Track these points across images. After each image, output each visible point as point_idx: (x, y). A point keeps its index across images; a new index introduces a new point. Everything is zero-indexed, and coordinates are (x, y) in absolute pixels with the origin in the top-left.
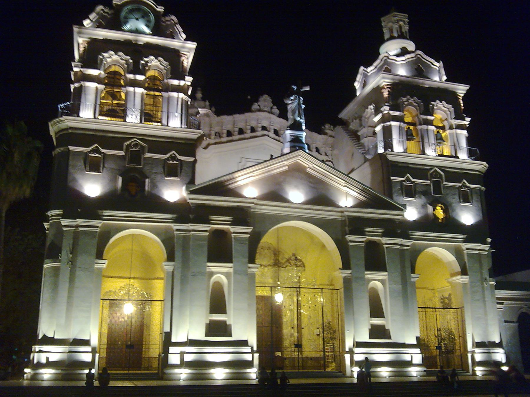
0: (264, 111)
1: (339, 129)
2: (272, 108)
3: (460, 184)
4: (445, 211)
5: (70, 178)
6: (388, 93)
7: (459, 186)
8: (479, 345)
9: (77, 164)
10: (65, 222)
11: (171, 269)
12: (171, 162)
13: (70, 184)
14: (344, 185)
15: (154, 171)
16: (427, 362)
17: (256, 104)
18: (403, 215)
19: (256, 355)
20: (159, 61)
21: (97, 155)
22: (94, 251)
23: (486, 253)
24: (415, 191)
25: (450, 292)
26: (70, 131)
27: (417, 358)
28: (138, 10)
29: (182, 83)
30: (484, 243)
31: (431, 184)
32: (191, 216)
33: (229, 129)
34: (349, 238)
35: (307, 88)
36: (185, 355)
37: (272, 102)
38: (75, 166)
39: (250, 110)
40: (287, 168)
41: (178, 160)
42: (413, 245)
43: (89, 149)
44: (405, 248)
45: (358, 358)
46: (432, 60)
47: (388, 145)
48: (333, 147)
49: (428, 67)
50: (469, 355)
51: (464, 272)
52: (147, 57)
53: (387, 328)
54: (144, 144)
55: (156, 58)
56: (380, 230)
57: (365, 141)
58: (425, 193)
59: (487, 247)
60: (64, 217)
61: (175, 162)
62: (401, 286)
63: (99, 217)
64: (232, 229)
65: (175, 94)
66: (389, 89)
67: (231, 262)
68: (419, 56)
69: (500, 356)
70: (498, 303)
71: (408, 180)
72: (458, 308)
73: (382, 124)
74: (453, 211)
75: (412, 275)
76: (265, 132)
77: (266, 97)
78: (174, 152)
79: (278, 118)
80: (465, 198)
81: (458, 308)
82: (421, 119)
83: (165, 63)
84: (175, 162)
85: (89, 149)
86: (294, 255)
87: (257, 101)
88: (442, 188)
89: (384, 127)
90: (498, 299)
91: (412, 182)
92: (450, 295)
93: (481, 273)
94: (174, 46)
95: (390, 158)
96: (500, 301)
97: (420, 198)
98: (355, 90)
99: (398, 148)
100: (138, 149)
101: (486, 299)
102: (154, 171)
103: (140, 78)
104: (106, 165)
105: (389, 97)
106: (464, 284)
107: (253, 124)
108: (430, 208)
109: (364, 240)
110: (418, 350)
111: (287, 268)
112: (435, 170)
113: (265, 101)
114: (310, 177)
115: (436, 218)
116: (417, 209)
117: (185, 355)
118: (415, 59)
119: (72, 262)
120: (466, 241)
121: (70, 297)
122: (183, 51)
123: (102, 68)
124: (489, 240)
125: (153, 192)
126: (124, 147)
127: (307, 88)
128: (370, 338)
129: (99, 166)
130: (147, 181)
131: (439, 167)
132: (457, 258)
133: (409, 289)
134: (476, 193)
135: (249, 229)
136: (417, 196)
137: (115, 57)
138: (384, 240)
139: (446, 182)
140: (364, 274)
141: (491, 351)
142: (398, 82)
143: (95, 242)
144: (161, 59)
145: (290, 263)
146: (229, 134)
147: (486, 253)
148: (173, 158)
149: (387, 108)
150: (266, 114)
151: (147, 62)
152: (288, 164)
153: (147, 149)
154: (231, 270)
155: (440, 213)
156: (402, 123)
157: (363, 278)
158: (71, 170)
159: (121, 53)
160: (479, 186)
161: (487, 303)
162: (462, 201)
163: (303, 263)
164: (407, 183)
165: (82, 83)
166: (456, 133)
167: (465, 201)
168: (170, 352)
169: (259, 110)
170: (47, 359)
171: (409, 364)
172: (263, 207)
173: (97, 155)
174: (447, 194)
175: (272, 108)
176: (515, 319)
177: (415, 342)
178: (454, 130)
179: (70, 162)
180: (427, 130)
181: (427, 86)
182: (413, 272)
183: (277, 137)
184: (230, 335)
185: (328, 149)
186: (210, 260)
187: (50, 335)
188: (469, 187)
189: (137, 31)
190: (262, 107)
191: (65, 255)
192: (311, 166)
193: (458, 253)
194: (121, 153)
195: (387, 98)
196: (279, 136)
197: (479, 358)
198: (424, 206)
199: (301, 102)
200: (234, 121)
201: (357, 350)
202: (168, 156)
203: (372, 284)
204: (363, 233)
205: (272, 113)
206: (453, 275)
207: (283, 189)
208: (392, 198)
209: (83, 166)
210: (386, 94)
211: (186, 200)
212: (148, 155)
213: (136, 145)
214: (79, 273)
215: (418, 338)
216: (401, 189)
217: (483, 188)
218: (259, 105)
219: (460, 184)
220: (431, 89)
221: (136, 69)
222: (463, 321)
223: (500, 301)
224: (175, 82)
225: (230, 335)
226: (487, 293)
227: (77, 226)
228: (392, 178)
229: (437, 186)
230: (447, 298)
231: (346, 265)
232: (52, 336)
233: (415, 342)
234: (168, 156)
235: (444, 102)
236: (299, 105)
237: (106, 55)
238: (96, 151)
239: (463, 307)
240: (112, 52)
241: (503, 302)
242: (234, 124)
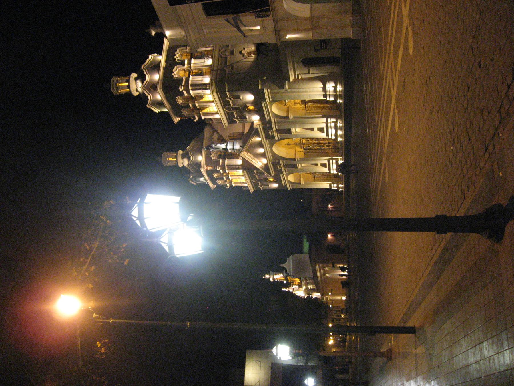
3: (230, 100)
9: (267, 188)
19: (333, 158)
20: (214, 175)
23: (269, 90)
30: (262, 91)
40: (249, 154)
44: (276, 121)
46: (149, 101)
59: (266, 92)
62: (297, 125)
94: (205, 173)
97: (245, 114)
109: (277, 134)
118: (153, 106)
120: (265, 100)
122: (205, 170)
123: (225, 183)
128: (324, 132)
131: (223, 108)
135: (281, 162)
147: (269, 90)
148: (256, 174)
151: (217, 177)
152: (246, 153)
156: (201, 115)
160: (227, 93)
162: (240, 99)
167: (239, 98)
172: (270, 158)
181: (170, 105)
184: (326, 164)
186: (297, 168)
189: (205, 179)
202: (256, 175)
212: (257, 178)
216: (243, 120)
225: (326, 164)
234: (256, 175)
237: (219, 184)
241: (297, 75)
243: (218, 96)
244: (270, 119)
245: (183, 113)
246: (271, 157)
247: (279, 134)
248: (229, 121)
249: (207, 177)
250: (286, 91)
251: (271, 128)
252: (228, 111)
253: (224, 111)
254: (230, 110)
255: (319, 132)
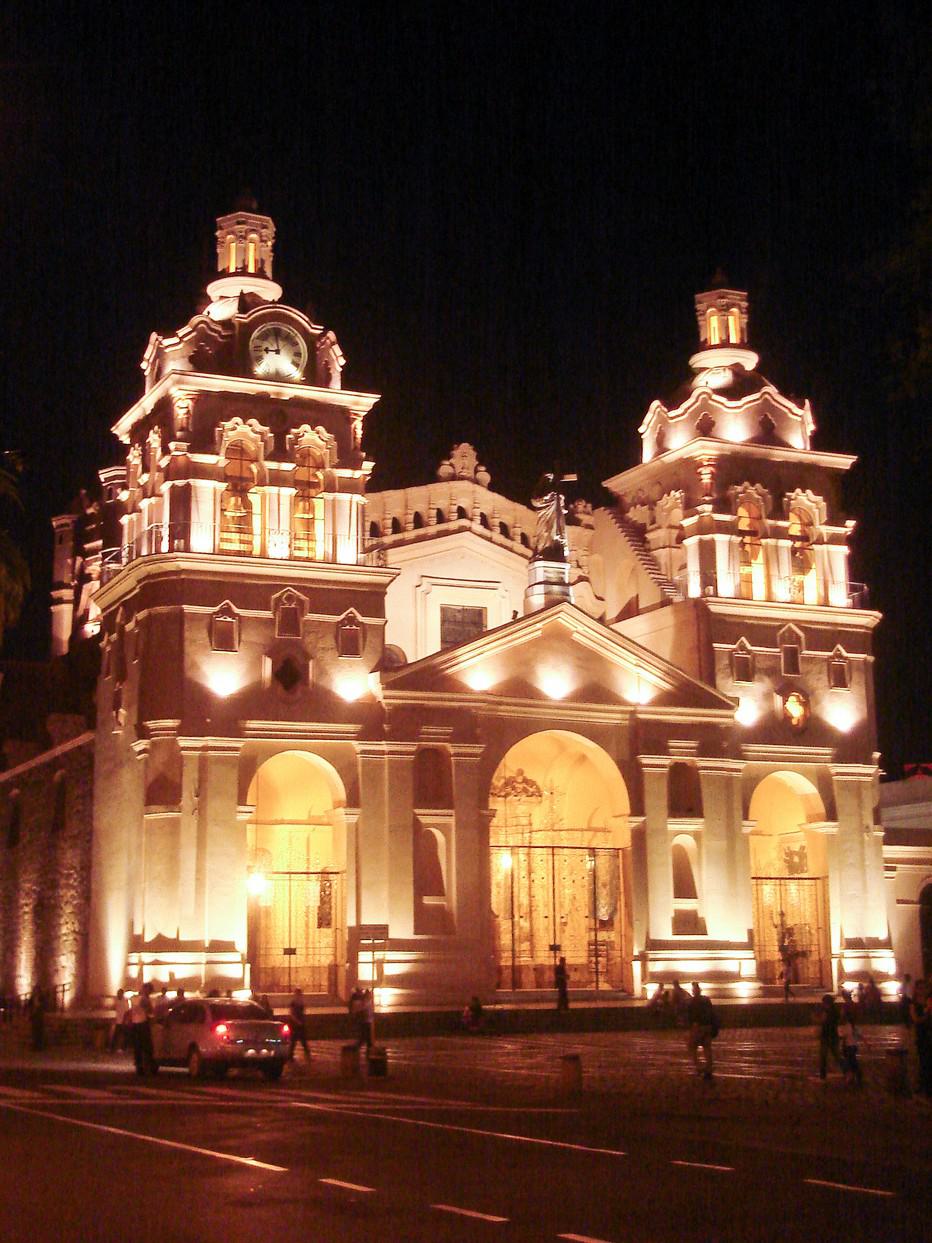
0: (462, 478)
1: (603, 517)
2: (476, 471)
3: (831, 654)
4: (806, 704)
5: (188, 662)
6: (710, 476)
7: (831, 657)
8: (854, 944)
9: (196, 639)
10: (183, 742)
11: (354, 819)
12: (348, 627)
13: (189, 674)
14: (634, 662)
15: (320, 645)
16: (764, 973)
17: (447, 463)
18: (732, 717)
21: (229, 619)
22: (234, 790)
24: (754, 666)
25: (804, 843)
26: (183, 576)
27: (749, 968)
28: (277, 334)
29: (357, 474)
30: (868, 761)
31: (782, 654)
32: (386, 727)
33: (397, 516)
34: (646, 760)
35: (573, 478)
36: (386, 966)
37: (478, 458)
38: (193, 641)
39: (436, 479)
40: (540, 632)
41: (359, 624)
42: (748, 768)
43: (217, 609)
44: (734, 774)
45: (655, 967)
47: (709, 579)
48: (591, 548)
49: (782, 417)
50: (834, 962)
51: (831, 814)
52: (297, 426)
53: (700, 915)
54: (303, 597)
55: (313, 429)
56: (693, 744)
57: (662, 555)
58: (771, 672)
59: (872, 769)
60: (182, 731)
61: (354, 627)
63: (239, 733)
64: (451, 749)
65: (345, 497)
66: (712, 469)
67: (450, 807)
68: (767, 396)
69: (885, 962)
70: (888, 869)
71: (743, 648)
72: (818, 878)
73: (698, 537)
74: (817, 703)
75: (745, 823)
76: (464, 522)
77: (465, 447)
78: (352, 609)
79: (490, 493)
80: (840, 680)
81: (818, 878)
82: (767, 526)
83: (326, 435)
84: (354, 627)
85: (217, 609)
86: (521, 772)
87: (449, 457)
88: (800, 659)
89: (701, 542)
90: (887, 861)
91: (749, 652)
92: (803, 848)
93: (861, 816)
95: (714, 608)
96: (890, 865)
97: (761, 680)
98: (637, 443)
99: (726, 585)
100: (293, 606)
101: (867, 863)
102: (320, 645)
103: (287, 466)
104: (243, 637)
105: (712, 483)
106: (831, 838)
107: (442, 504)
108: (778, 699)
110: (749, 954)
111: (509, 798)
112: (790, 630)
113: (464, 457)
114: (577, 647)
115: (788, 718)
116: (756, 701)
117: (386, 966)
119: (200, 810)
120: (839, 759)
121: (200, 871)
124: (877, 755)
125: (321, 683)
126: (272, 603)
127: (573, 478)
128: (676, 932)
129: (231, 638)
130: (311, 663)
131: (797, 623)
132: (821, 790)
133: (739, 847)
134: (858, 669)
135: (478, 749)
136: (756, 677)
137: (243, 428)
138: (701, 762)
139: (807, 650)
140: (666, 823)
141: (871, 955)
142: (729, 453)
143: (233, 776)
144: (320, 428)
145: (514, 788)
146: (397, 527)
147: (869, 779)
149: (708, 508)
150: (466, 484)
151: (297, 436)
153: (307, 606)
154: (452, 821)
155: (795, 709)
157: (664, 831)
158: (189, 648)
159: (253, 421)
160: (863, 656)
161: (868, 870)
163: (538, 788)
164: (741, 654)
165: (192, 481)
166: (828, 552)
168: (360, 960)
169: (453, 478)
170: (172, 975)
171: (734, 977)
173: (229, 619)
174: (808, 673)
175: (476, 471)
176: (915, 897)
177: (744, 938)
178: (825, 546)
179: (187, 634)
180: (777, 548)
182: (746, 817)
183: (486, 532)
185: (581, 552)
187: (171, 934)
188: (846, 658)
189: (278, 378)
190: (458, 470)
191: (188, 799)
192: (581, 628)
193: (825, 784)
194: (268, 614)
195: (709, 486)
196: (491, 530)
197: (852, 964)
198: (768, 697)
199: (562, 504)
200: (406, 501)
201: (652, 954)
202: (343, 616)
203: (679, 840)
204: (663, 750)
205: (476, 482)
206: (812, 819)
207: (531, 671)
208: (714, 686)
209: (207, 639)
210: (706, 479)
211: (373, 698)
213: (290, 598)
214: (212, 829)
215: (750, 933)
216: (731, 665)
217: (871, 659)
218: (451, 465)
219: (831, 654)
220: (786, 465)
221: (280, 452)
222: (826, 902)
223: (890, 865)
224: (346, 473)
226: (869, 852)
227: (205, 748)
228: (715, 645)
229: (792, 658)
230: (796, 853)
231: (638, 808)
232: (174, 936)
233: (744, 938)
234: (343, 616)
235: (809, 492)
236: (558, 509)
237: (228, 425)
238: (227, 611)
239: (827, 877)
240: (238, 420)
242: (406, 506)
243: (823, 623)
244: (745, 758)
245: (746, 484)
246: (509, 711)
247: (665, 770)
248: (728, 619)
249: (289, 392)
250: (867, 827)
251: (703, 752)
252: (781, 631)
253: (788, 621)
254: (783, 640)
255: (673, 914)
